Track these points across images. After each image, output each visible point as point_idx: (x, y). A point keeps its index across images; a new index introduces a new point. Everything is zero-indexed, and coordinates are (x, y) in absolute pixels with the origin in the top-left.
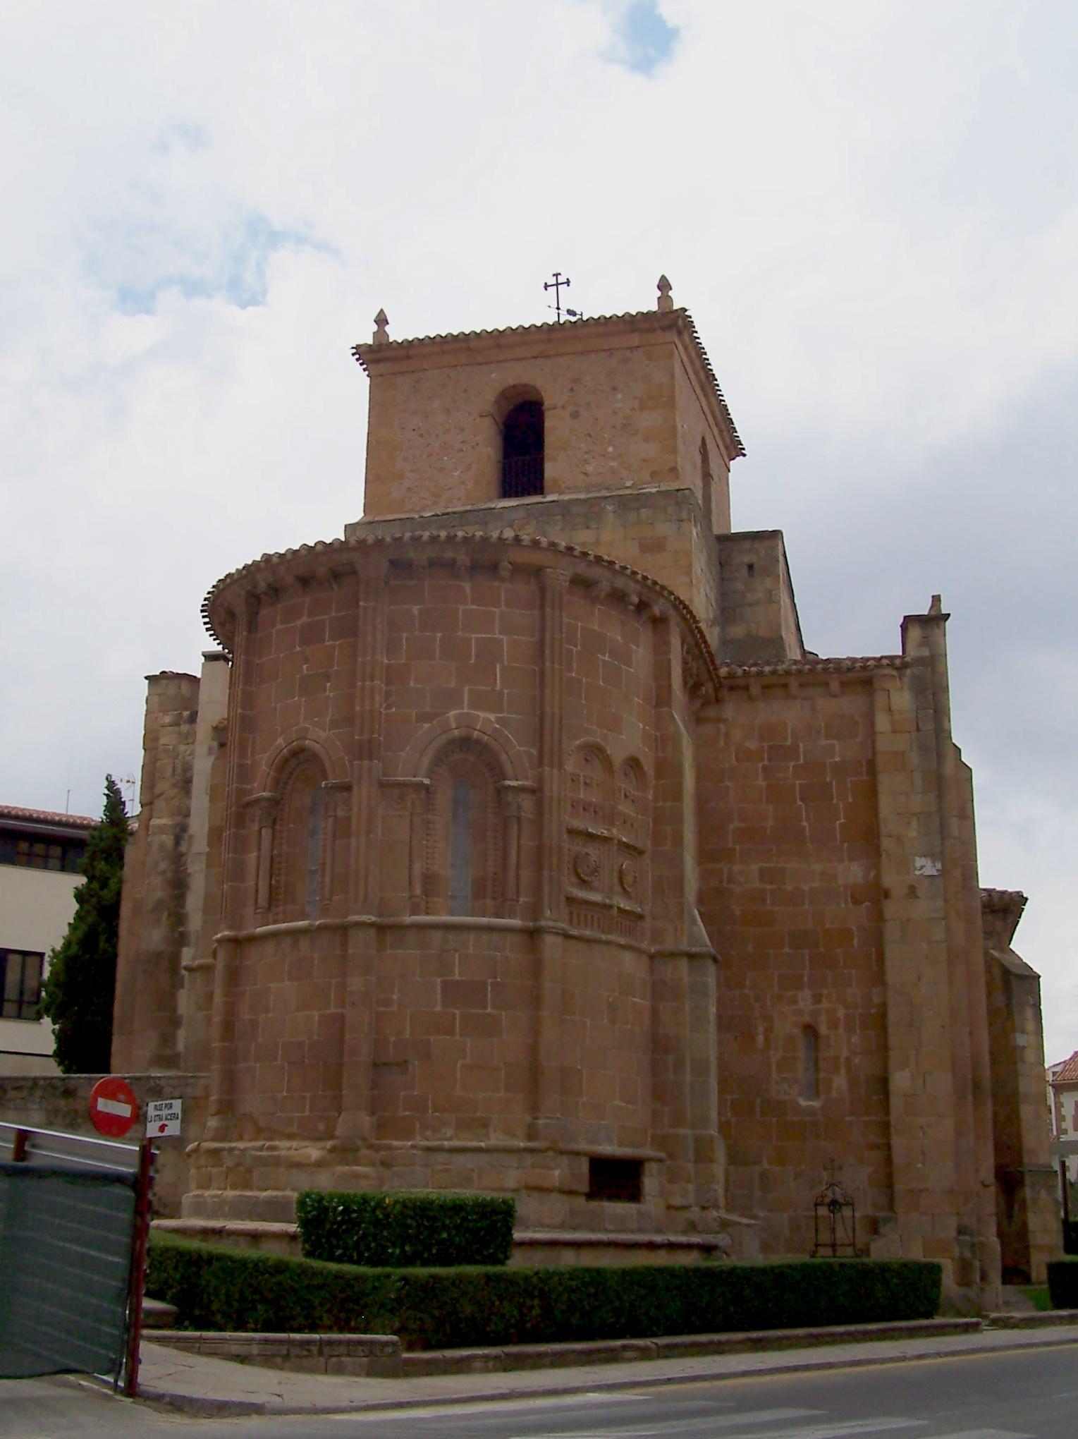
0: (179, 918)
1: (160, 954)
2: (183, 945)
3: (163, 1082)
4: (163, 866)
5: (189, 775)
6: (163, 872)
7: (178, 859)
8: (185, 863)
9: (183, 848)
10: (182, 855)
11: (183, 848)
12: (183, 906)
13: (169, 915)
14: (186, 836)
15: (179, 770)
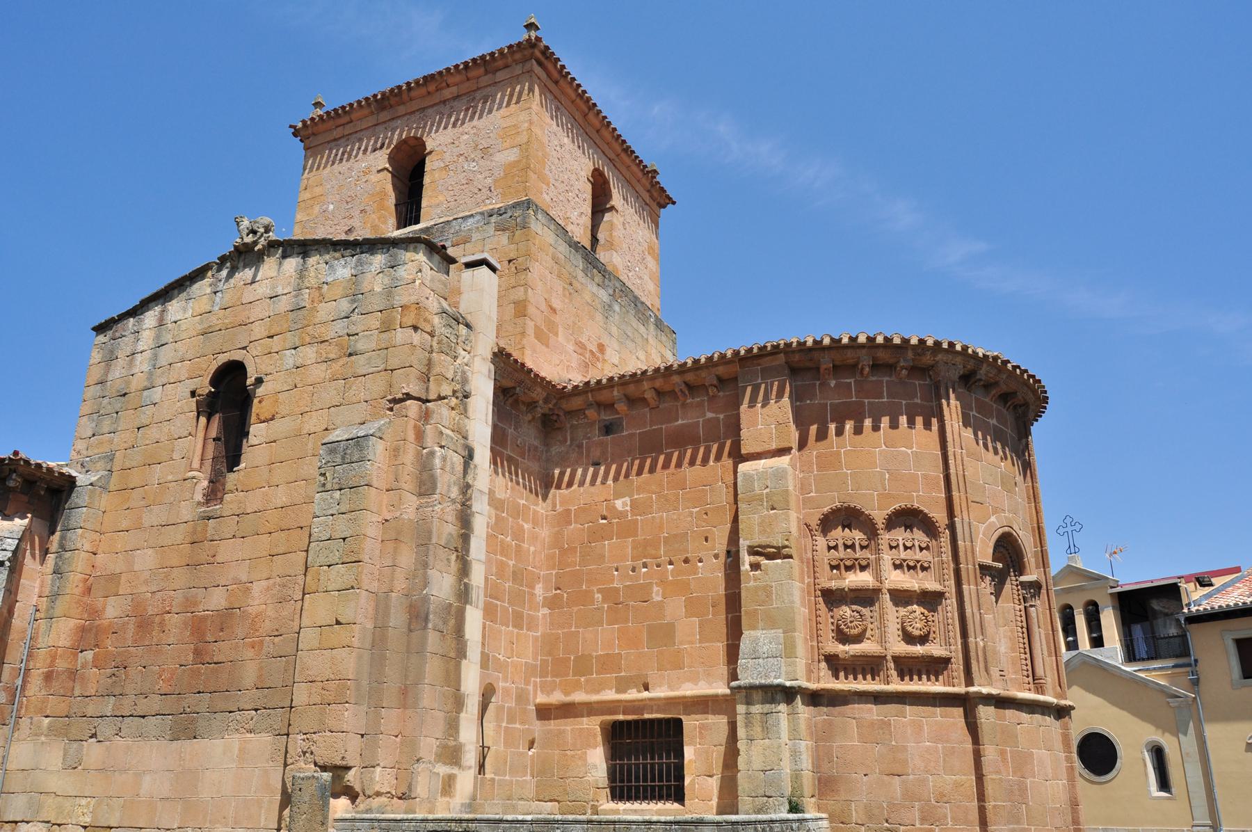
9: (469, 479)
11: (469, 479)
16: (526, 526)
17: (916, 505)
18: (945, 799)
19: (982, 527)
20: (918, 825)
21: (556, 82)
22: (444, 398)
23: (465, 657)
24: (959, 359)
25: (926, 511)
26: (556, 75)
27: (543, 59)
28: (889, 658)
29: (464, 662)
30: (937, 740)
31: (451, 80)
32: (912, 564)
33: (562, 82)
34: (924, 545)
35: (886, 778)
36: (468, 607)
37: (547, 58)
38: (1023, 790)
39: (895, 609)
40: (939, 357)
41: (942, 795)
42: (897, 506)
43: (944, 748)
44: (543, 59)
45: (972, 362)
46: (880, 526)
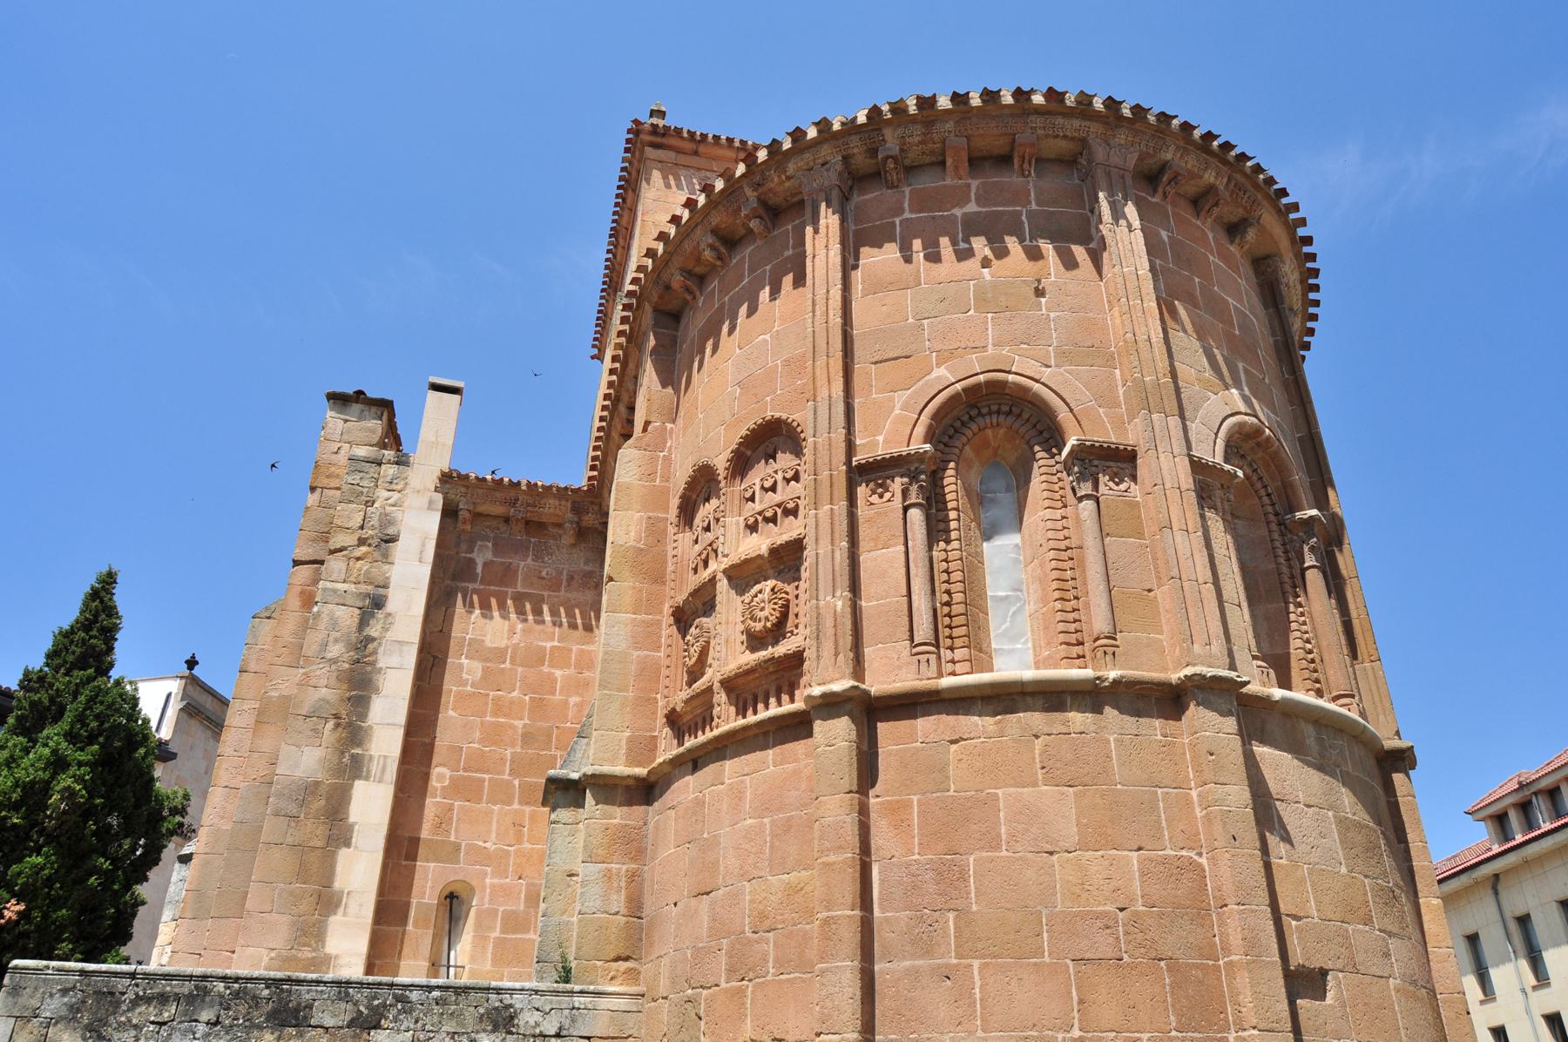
0: (352, 732)
1: (312, 788)
2: (359, 777)
3: (518, 1001)
4: (335, 650)
5: (391, 531)
6: (334, 661)
7: (363, 646)
8: (375, 652)
9: (373, 630)
10: (371, 639)
11: (373, 630)
12: (363, 716)
13: (337, 725)
14: (380, 614)
15: (375, 522)
16: (558, 673)
17: (769, 415)
18: (767, 924)
19: (901, 397)
20: (723, 985)
21: (696, 153)
22: (340, 550)
23: (348, 844)
24: (825, 151)
25: (784, 416)
26: (688, 146)
27: (659, 140)
28: (717, 686)
29: (343, 854)
30: (762, 810)
31: (624, 222)
32: (769, 514)
33: (702, 149)
34: (790, 474)
35: (693, 902)
36: (359, 787)
37: (664, 135)
38: (950, 877)
39: (739, 599)
40: (791, 167)
41: (763, 916)
42: (744, 432)
43: (773, 822)
44: (659, 140)
45: (855, 141)
46: (722, 473)
